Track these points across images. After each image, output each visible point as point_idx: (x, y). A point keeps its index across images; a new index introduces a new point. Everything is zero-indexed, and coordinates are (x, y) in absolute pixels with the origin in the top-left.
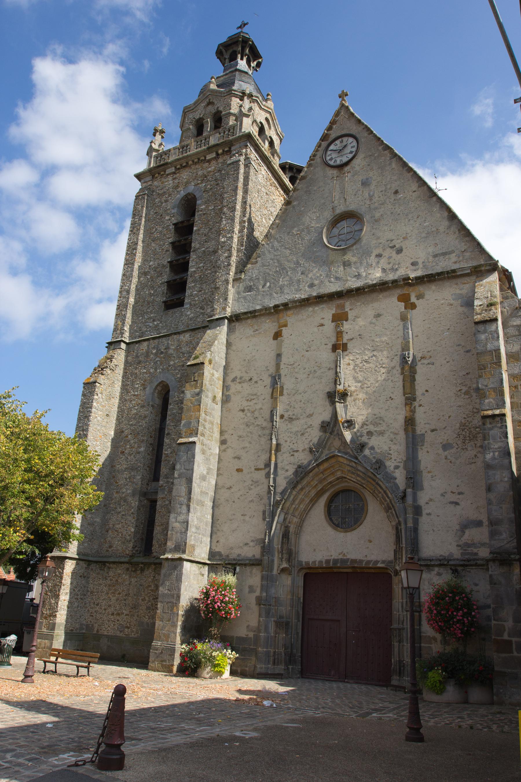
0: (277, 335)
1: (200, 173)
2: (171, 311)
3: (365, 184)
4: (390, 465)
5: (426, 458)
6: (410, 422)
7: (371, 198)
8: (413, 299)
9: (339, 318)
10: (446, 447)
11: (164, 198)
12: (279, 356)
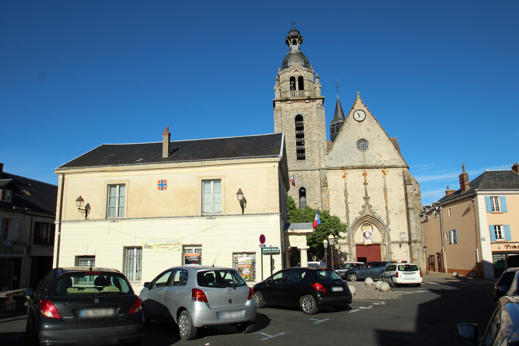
0: (344, 177)
1: (303, 107)
2: (300, 161)
3: (368, 130)
4: (382, 218)
5: (391, 216)
6: (386, 207)
7: (371, 135)
8: (386, 172)
9: (365, 175)
10: (396, 214)
11: (288, 114)
12: (345, 184)
